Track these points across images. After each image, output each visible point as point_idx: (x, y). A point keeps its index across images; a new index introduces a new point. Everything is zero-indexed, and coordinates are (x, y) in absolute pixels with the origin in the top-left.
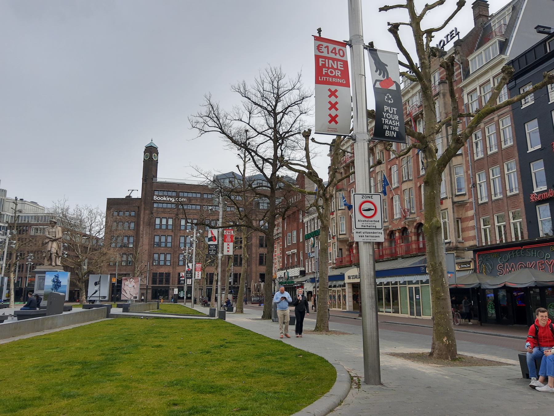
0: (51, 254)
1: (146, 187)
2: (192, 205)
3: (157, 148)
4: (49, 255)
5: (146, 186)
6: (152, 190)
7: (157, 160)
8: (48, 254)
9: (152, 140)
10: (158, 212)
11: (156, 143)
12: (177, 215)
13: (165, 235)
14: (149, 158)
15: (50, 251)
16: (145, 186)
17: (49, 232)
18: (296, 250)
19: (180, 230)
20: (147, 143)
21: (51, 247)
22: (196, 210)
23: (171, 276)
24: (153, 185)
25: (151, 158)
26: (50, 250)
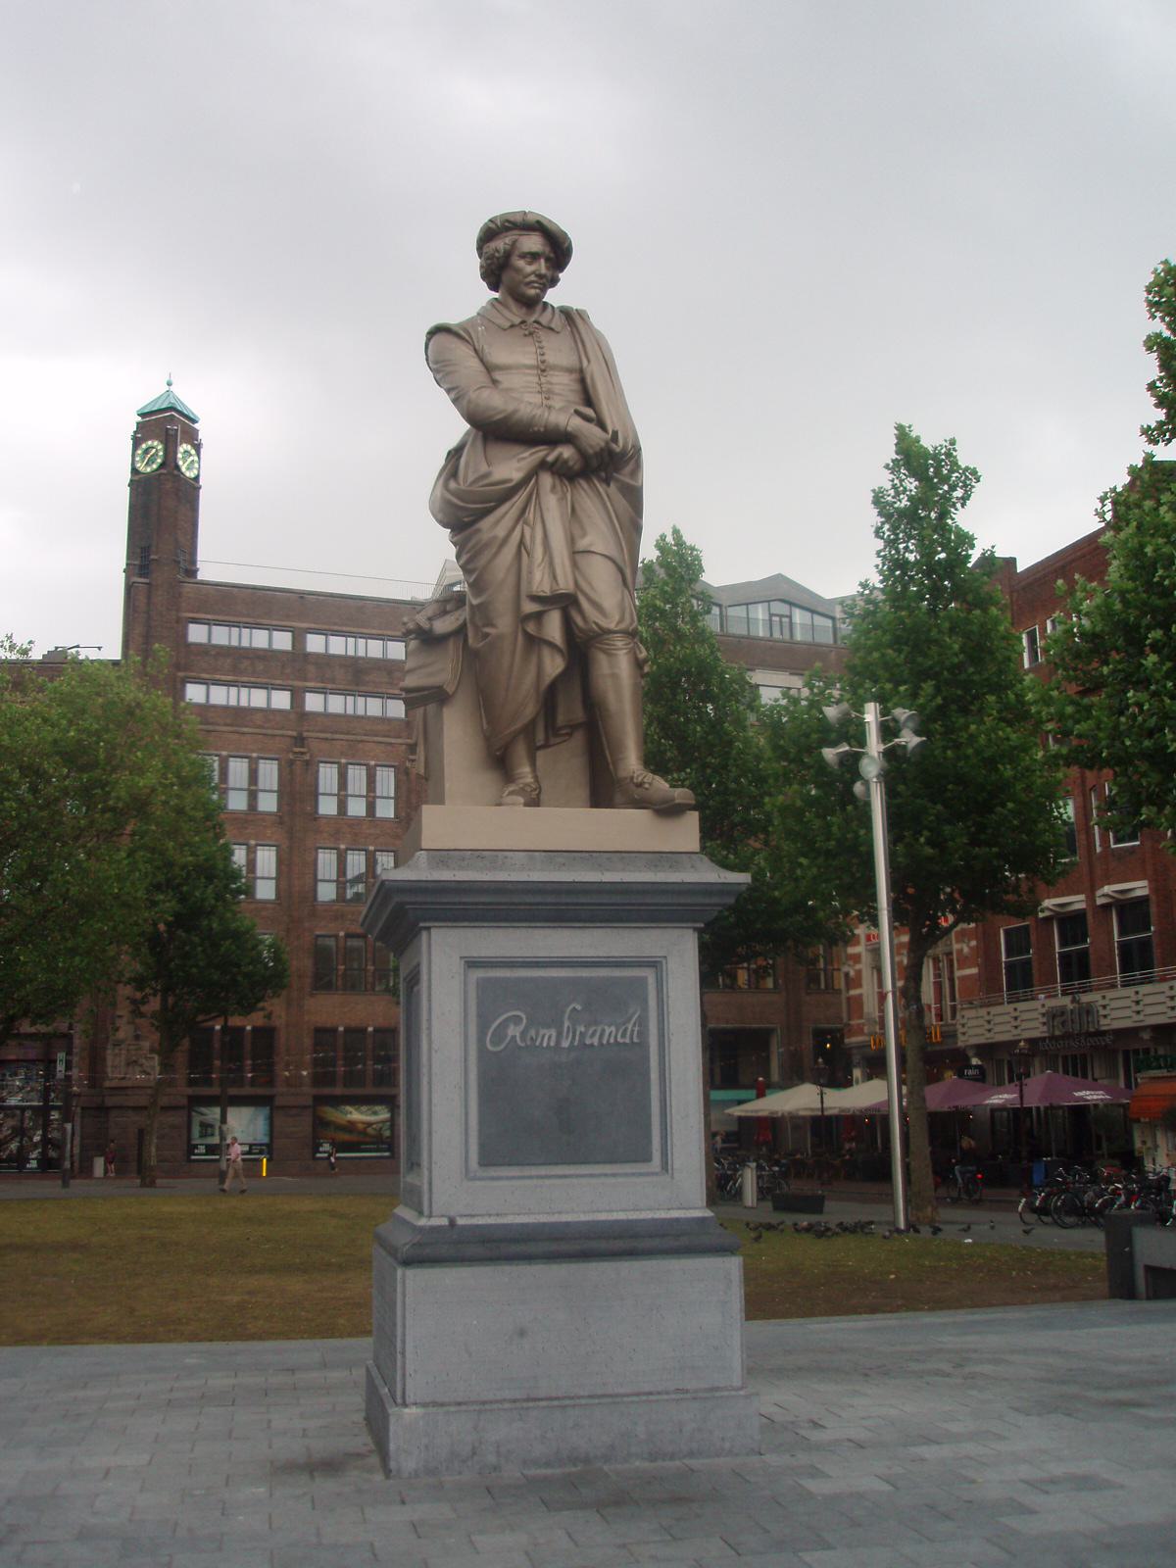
0: (581, 648)
1: (148, 604)
2: (366, 695)
3: (194, 421)
4: (554, 665)
5: (149, 597)
6: (178, 620)
7: (197, 478)
8: (534, 642)
9: (169, 384)
10: (211, 728)
11: (190, 399)
12: (300, 740)
13: (245, 842)
14: (162, 466)
15: (566, 603)
16: (142, 599)
17: (489, 368)
18: (1082, 897)
19: (314, 816)
20: (147, 394)
21: (575, 553)
22: (383, 720)
23: (282, 1039)
24: (180, 594)
25: (170, 463)
26: (565, 585)
